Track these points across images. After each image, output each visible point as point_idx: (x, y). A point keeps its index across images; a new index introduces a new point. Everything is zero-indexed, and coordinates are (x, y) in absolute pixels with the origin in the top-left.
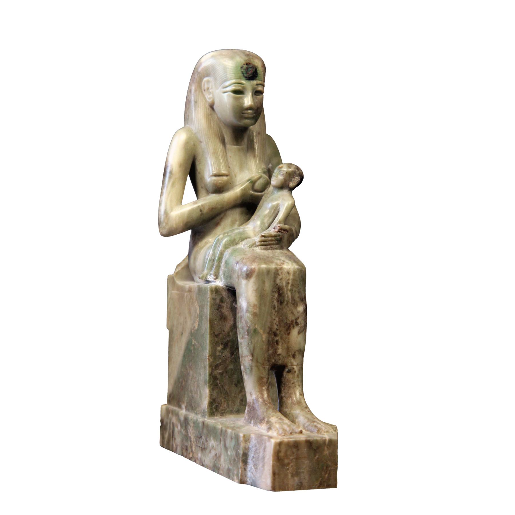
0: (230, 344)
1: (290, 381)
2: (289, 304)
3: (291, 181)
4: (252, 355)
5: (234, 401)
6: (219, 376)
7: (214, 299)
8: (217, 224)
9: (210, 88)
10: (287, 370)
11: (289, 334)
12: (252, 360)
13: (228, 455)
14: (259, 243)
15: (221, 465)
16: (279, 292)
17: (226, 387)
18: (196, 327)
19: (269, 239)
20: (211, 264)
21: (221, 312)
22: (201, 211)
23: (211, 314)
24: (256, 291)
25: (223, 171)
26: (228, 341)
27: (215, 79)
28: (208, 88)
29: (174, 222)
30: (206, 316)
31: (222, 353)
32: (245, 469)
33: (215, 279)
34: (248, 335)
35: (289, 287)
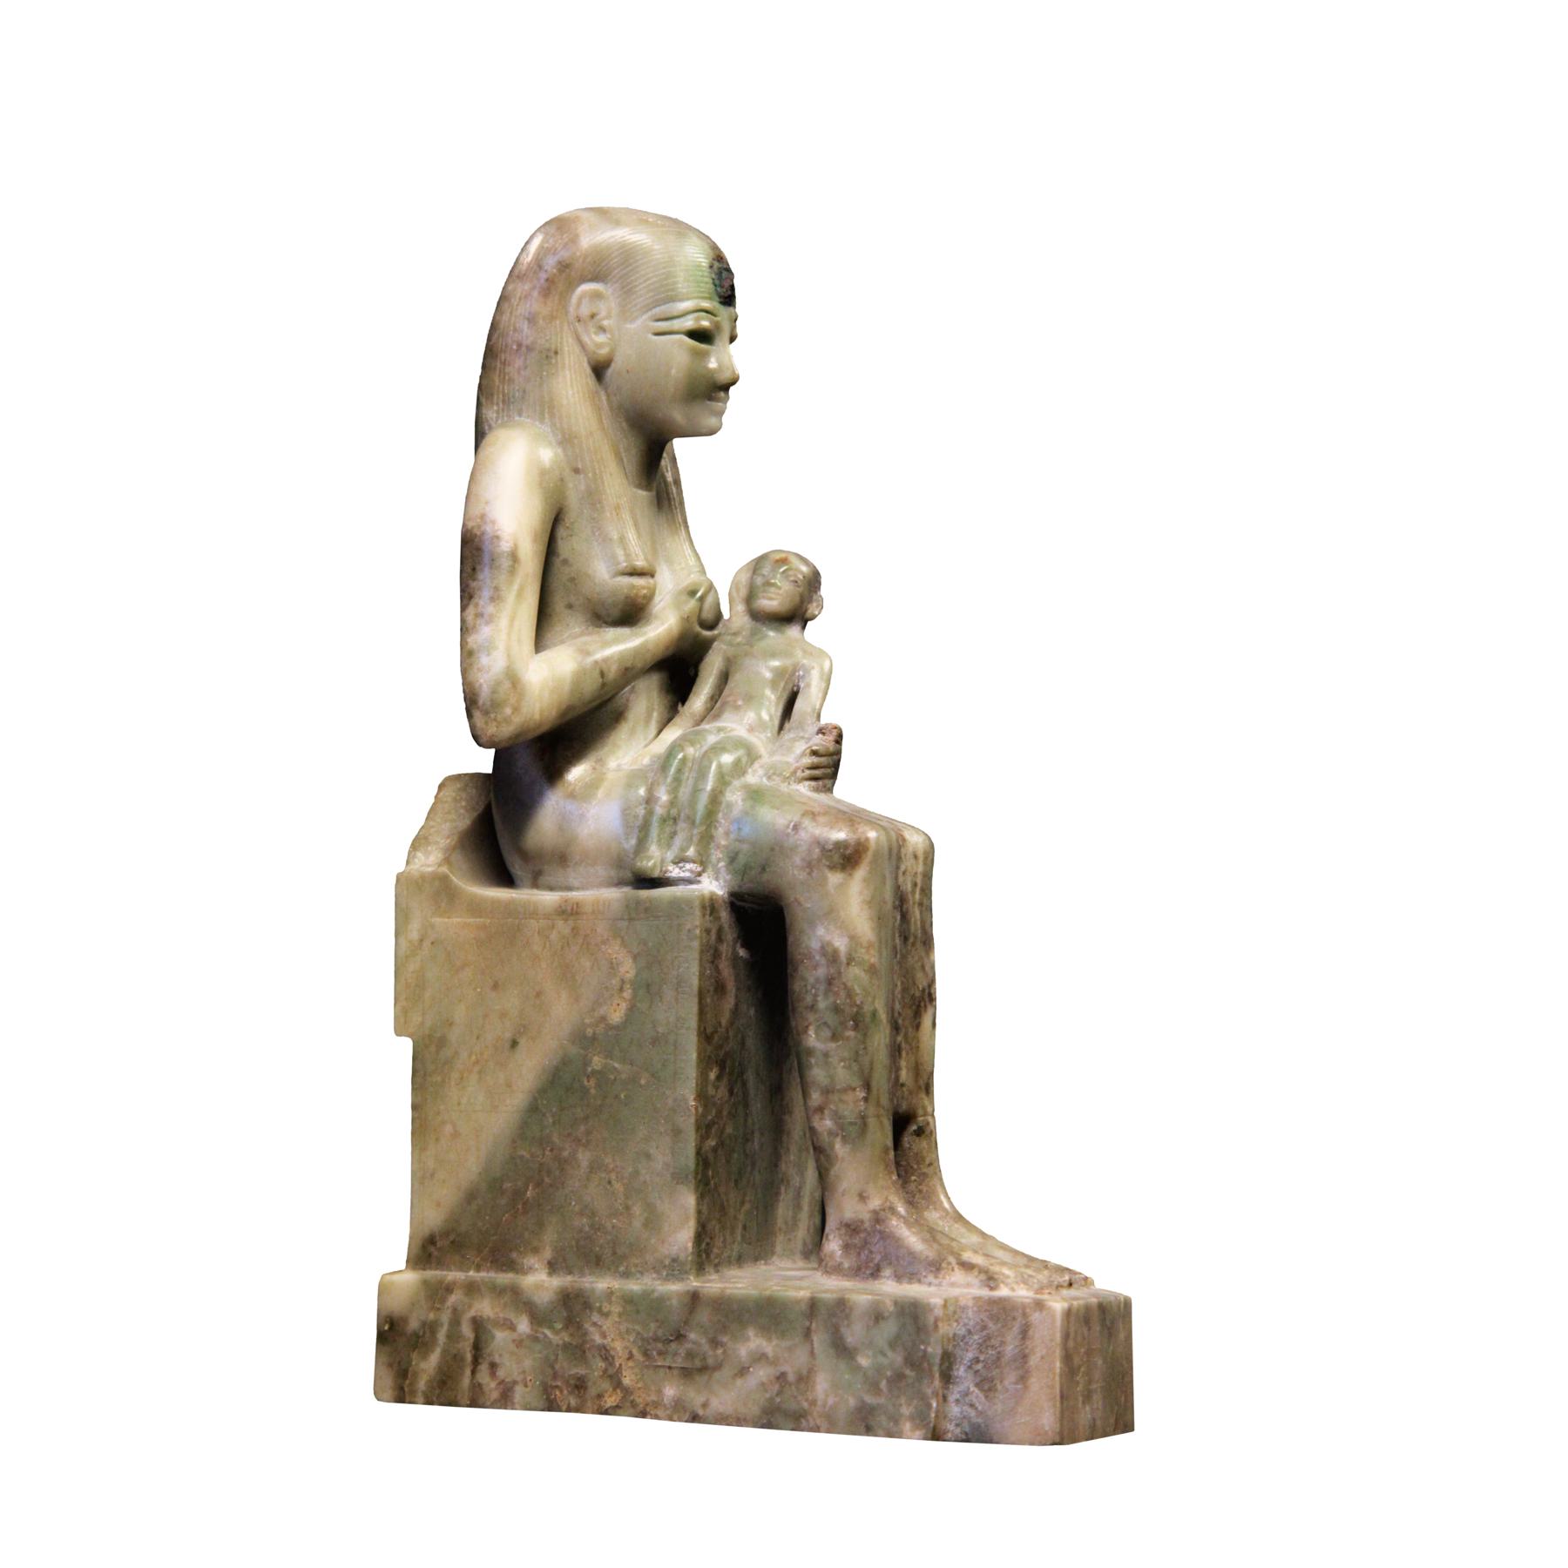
0: (728, 1063)
1: (923, 1159)
2: (919, 944)
3: (810, 601)
4: (867, 1086)
5: (732, 1233)
6: (711, 1156)
7: (708, 931)
8: (618, 717)
9: (603, 314)
10: (914, 1127)
11: (918, 1027)
12: (866, 1099)
13: (859, 1368)
14: (808, 772)
15: (813, 1403)
16: (901, 906)
17: (722, 1189)
18: (616, 1016)
19: (823, 760)
20: (668, 830)
21: (717, 968)
22: (602, 674)
23: (702, 975)
24: (870, 903)
25: (640, 563)
26: (727, 1054)
27: (627, 291)
28: (593, 316)
29: (538, 705)
30: (680, 983)
31: (717, 1088)
32: (945, 1398)
33: (700, 874)
34: (856, 1027)
35: (917, 896)
